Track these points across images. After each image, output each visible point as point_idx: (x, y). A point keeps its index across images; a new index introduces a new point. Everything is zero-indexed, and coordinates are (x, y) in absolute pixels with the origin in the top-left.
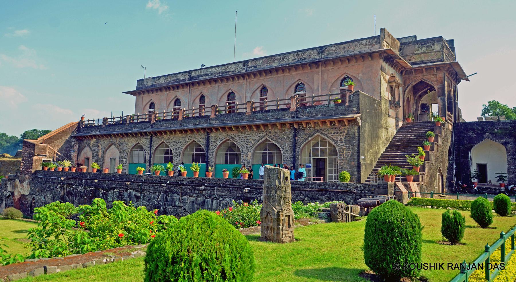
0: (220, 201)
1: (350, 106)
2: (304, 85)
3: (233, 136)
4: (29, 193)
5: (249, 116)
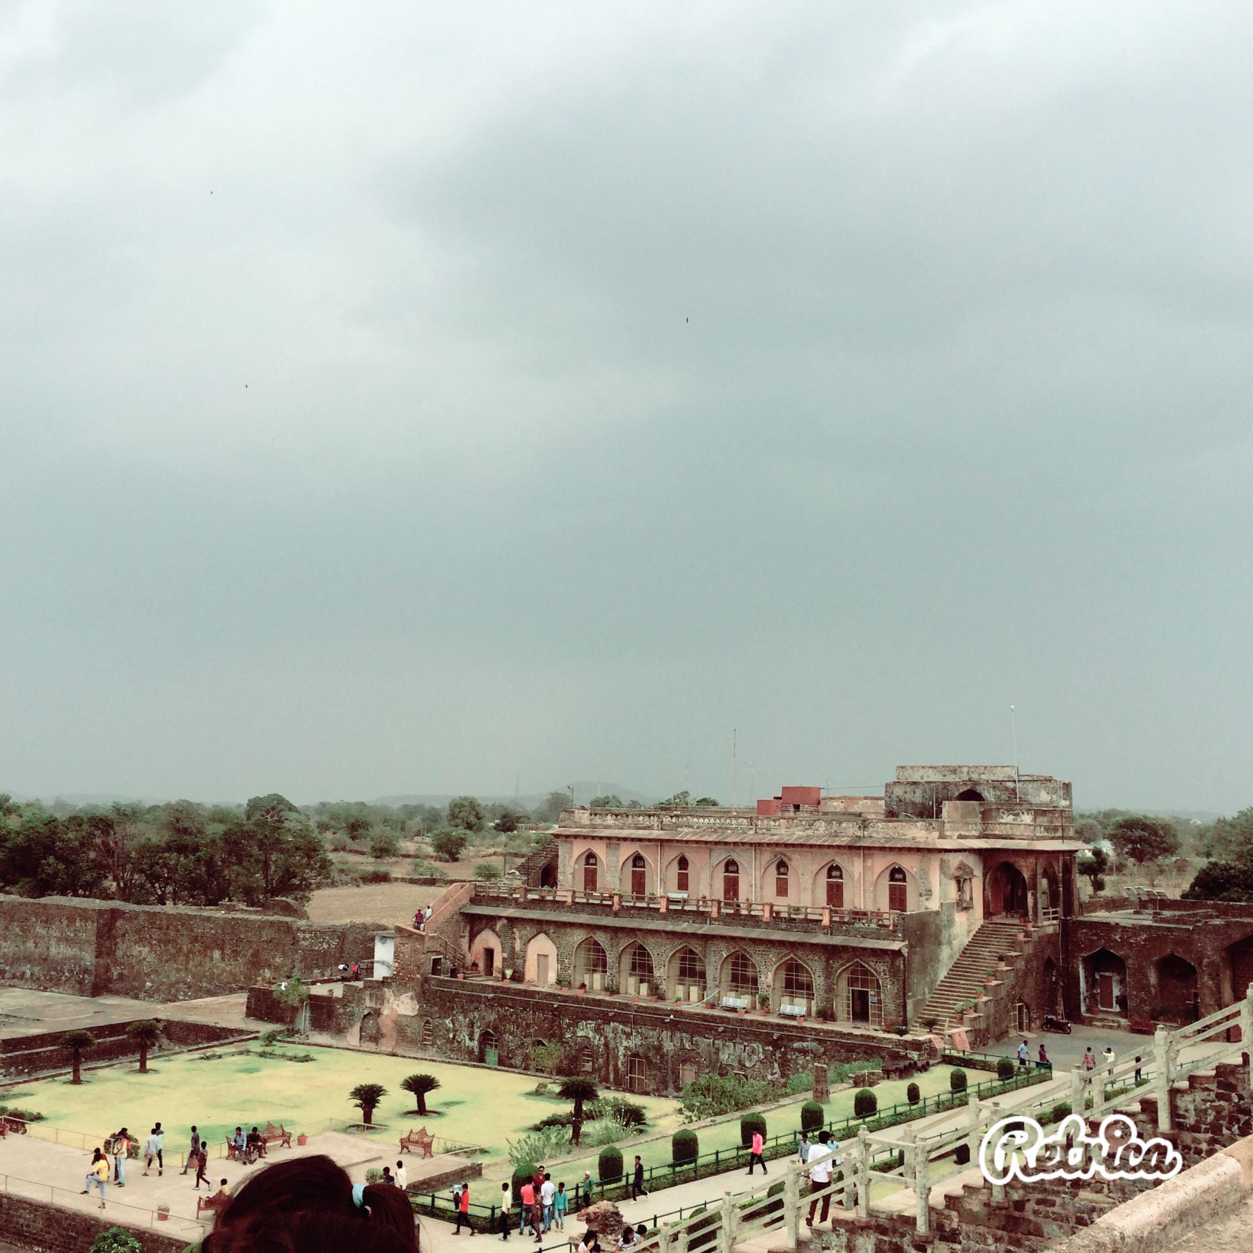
0: (745, 1046)
1: (894, 931)
2: (841, 872)
3: (746, 947)
5: (767, 923)
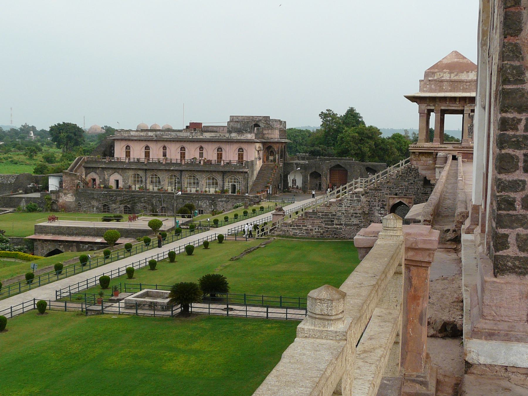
2: (222, 150)
4: (74, 200)
